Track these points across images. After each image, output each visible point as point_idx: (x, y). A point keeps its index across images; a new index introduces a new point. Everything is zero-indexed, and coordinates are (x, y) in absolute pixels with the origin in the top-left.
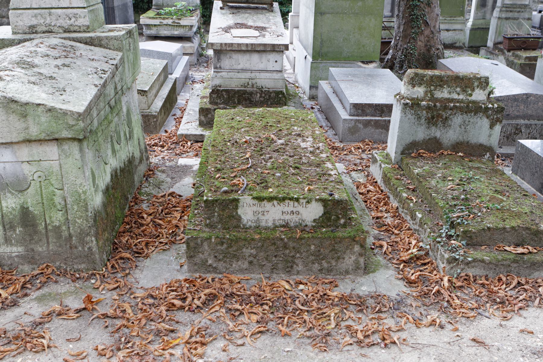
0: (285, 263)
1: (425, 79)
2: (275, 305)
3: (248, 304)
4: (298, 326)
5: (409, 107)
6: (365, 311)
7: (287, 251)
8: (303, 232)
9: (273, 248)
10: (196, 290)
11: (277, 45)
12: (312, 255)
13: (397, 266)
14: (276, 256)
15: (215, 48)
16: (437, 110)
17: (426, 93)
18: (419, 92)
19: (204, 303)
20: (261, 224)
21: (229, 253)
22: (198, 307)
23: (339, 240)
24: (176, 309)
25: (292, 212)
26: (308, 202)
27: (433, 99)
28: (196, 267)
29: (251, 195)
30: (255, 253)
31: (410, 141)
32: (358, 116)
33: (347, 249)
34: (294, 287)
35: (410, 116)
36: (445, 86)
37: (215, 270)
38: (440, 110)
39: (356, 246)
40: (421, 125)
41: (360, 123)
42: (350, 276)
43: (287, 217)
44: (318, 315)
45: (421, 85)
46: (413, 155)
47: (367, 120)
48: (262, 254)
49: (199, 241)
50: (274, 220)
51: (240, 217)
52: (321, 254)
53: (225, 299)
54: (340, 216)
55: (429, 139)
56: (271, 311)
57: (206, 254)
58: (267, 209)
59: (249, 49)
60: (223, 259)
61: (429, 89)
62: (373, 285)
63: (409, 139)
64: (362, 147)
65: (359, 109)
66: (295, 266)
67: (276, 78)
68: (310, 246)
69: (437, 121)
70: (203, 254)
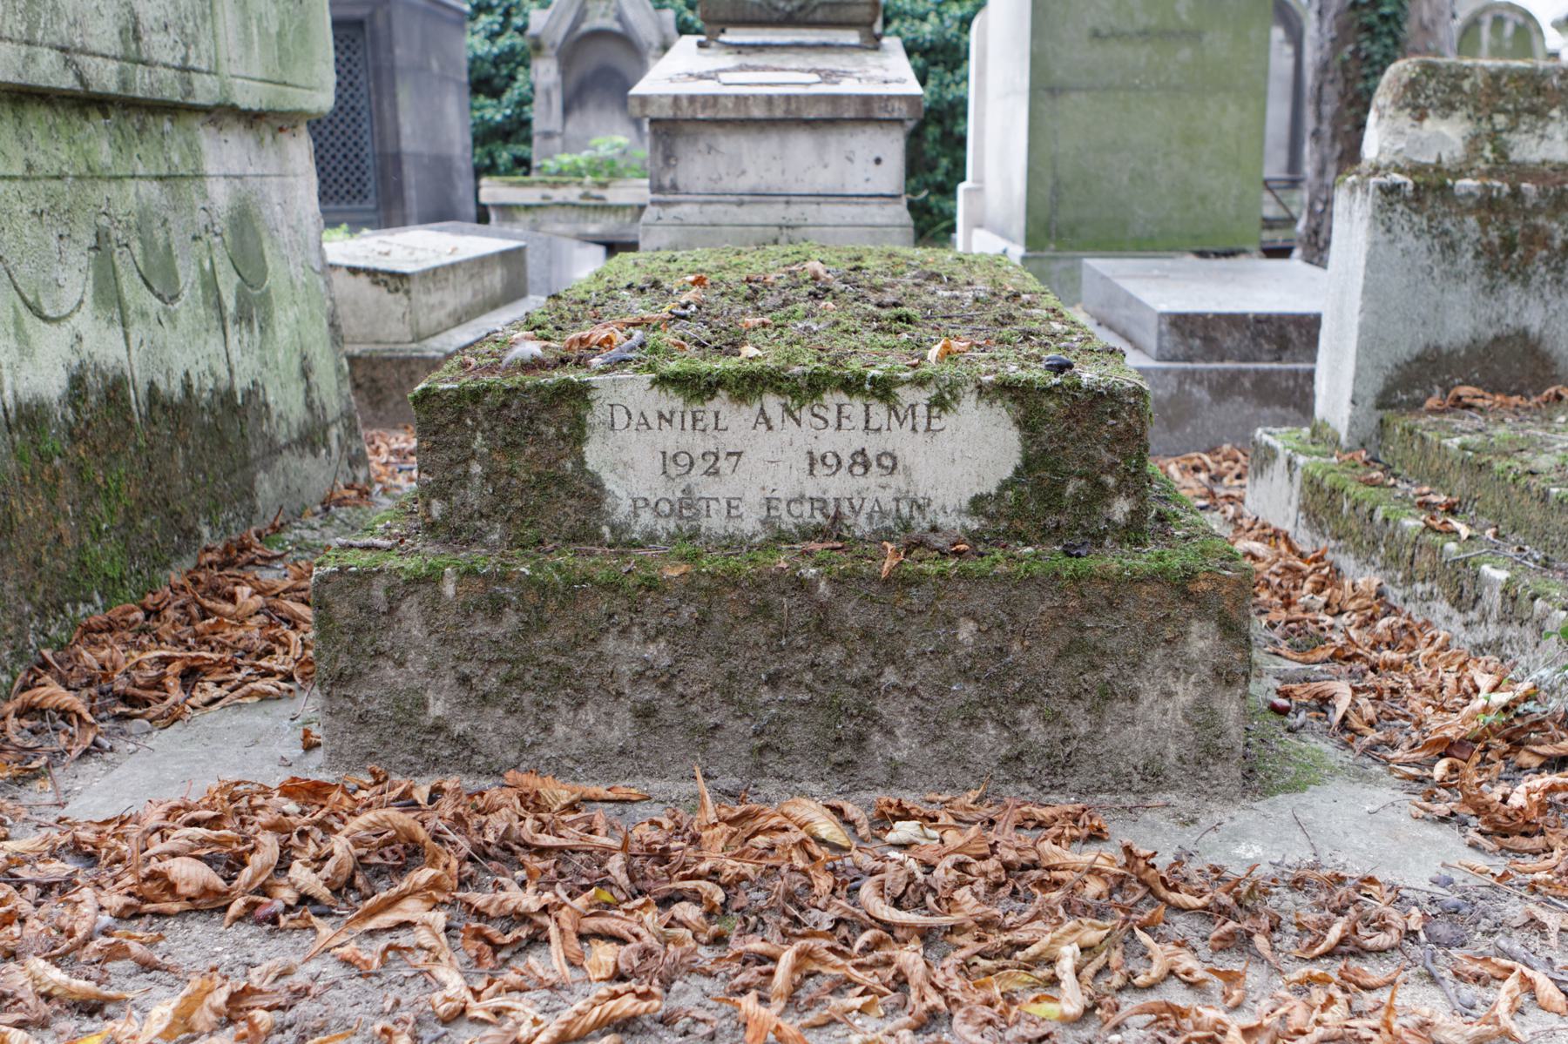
0: (821, 717)
1: (1466, 85)
2: (741, 900)
3: (586, 888)
4: (858, 1002)
5: (1406, 201)
6: (1260, 941)
7: (834, 654)
8: (916, 553)
9: (756, 633)
10: (321, 824)
11: (880, 97)
12: (964, 673)
13: (1413, 771)
14: (773, 681)
15: (654, 112)
16: (1527, 213)
17: (1473, 143)
18: (1444, 139)
19: (343, 887)
20: (704, 523)
21: (529, 659)
22: (305, 899)
23: (1105, 589)
24: (176, 907)
25: (861, 460)
26: (940, 403)
27: (1503, 164)
28: (367, 738)
29: (651, 368)
30: (666, 661)
31: (1416, 350)
32: (1189, 359)
33: (1149, 646)
34: (864, 831)
35: (1409, 240)
36: (1555, 113)
37: (465, 752)
38: (1537, 210)
39: (1195, 627)
40: (1460, 277)
41: (1200, 383)
42: (1171, 797)
43: (837, 486)
44: (983, 956)
45: (1452, 107)
46: (1431, 403)
47: (1226, 371)
48: (701, 666)
49: (379, 593)
50: (769, 503)
51: (596, 483)
52: (1010, 671)
53: (468, 868)
54: (1111, 481)
55: (1497, 339)
56: (714, 928)
57: (417, 664)
58: (730, 441)
59: (779, 113)
60: (500, 694)
61: (1486, 126)
62: (1300, 837)
63: (1408, 344)
64: (1212, 466)
65: (1192, 334)
66: (877, 737)
67: (879, 220)
68: (951, 622)
69: (1526, 260)
70: (400, 664)
